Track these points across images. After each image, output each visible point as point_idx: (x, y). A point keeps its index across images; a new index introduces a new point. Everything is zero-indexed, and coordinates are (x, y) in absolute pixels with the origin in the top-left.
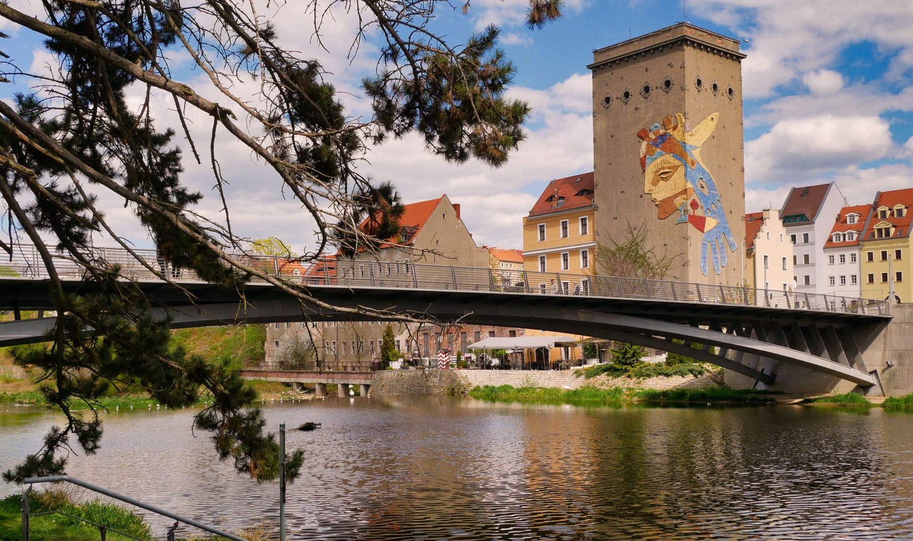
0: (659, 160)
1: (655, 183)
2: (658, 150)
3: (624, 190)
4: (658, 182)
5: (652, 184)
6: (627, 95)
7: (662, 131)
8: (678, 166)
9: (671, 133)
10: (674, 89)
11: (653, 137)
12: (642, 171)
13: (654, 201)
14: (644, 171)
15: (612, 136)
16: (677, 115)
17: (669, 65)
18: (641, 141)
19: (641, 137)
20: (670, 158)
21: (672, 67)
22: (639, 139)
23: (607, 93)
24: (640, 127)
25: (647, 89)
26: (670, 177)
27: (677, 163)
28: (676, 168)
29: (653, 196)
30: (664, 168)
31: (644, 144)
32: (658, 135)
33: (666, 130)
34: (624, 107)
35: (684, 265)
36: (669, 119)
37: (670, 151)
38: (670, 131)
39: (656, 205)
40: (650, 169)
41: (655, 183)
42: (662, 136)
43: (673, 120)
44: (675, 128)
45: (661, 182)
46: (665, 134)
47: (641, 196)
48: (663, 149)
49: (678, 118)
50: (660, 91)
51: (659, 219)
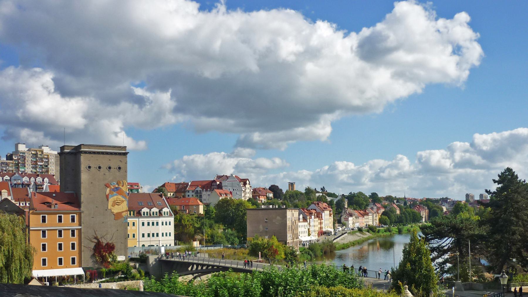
0: (115, 197)
1: (113, 206)
2: (115, 193)
3: (98, 206)
4: (115, 205)
5: (112, 206)
6: (100, 168)
7: (117, 186)
8: (124, 201)
9: (121, 188)
10: (122, 170)
11: (113, 187)
12: (107, 200)
13: (113, 213)
14: (108, 200)
15: (92, 183)
16: (124, 181)
17: (120, 161)
18: (107, 188)
19: (107, 186)
20: (120, 197)
21: (121, 162)
22: (105, 187)
23: (89, 164)
24: (106, 182)
25: (110, 168)
26: (120, 204)
27: (124, 199)
28: (123, 201)
29: (113, 211)
30: (117, 201)
31: (108, 190)
32: (115, 187)
33: (118, 185)
34: (98, 171)
35: (126, 239)
36: (120, 182)
37: (120, 195)
38: (121, 187)
39: (114, 214)
40: (111, 200)
41: (113, 206)
42: (117, 188)
43: (121, 182)
44: (123, 186)
45: (116, 205)
46: (118, 187)
47: (106, 210)
48: (117, 193)
49: (124, 182)
50: (116, 169)
51: (115, 220)
